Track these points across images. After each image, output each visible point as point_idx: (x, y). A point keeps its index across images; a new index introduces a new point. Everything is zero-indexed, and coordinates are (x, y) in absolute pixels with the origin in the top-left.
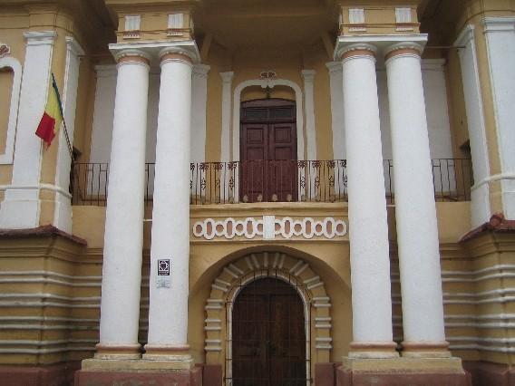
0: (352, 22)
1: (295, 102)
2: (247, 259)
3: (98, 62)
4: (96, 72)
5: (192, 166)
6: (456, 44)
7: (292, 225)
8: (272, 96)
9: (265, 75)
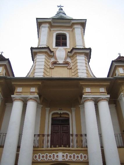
1: (69, 118)
3: (7, 103)
4: (6, 105)
5: (35, 135)
6: (119, 98)
7: (69, 156)
8: (62, 116)
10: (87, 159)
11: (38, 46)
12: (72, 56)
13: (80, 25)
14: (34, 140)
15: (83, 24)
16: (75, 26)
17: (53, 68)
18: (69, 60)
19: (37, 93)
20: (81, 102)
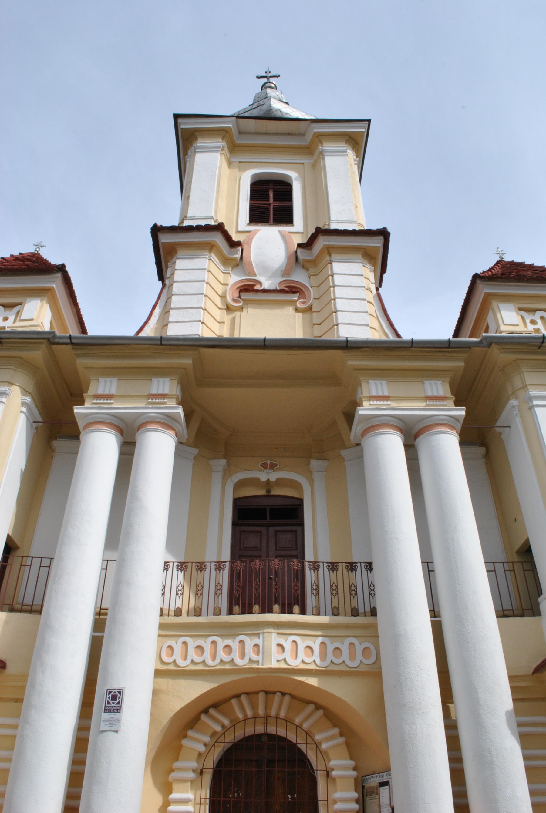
0: (374, 393)
1: (301, 500)
2: (234, 701)
3: (56, 439)
8: (275, 492)
9: (265, 466)
10: (372, 660)
11: (180, 224)
12: (314, 262)
13: (343, 144)
14: (164, 586)
15: (355, 137)
16: (327, 146)
17: (241, 309)
18: (300, 277)
19: (177, 399)
20: (349, 435)
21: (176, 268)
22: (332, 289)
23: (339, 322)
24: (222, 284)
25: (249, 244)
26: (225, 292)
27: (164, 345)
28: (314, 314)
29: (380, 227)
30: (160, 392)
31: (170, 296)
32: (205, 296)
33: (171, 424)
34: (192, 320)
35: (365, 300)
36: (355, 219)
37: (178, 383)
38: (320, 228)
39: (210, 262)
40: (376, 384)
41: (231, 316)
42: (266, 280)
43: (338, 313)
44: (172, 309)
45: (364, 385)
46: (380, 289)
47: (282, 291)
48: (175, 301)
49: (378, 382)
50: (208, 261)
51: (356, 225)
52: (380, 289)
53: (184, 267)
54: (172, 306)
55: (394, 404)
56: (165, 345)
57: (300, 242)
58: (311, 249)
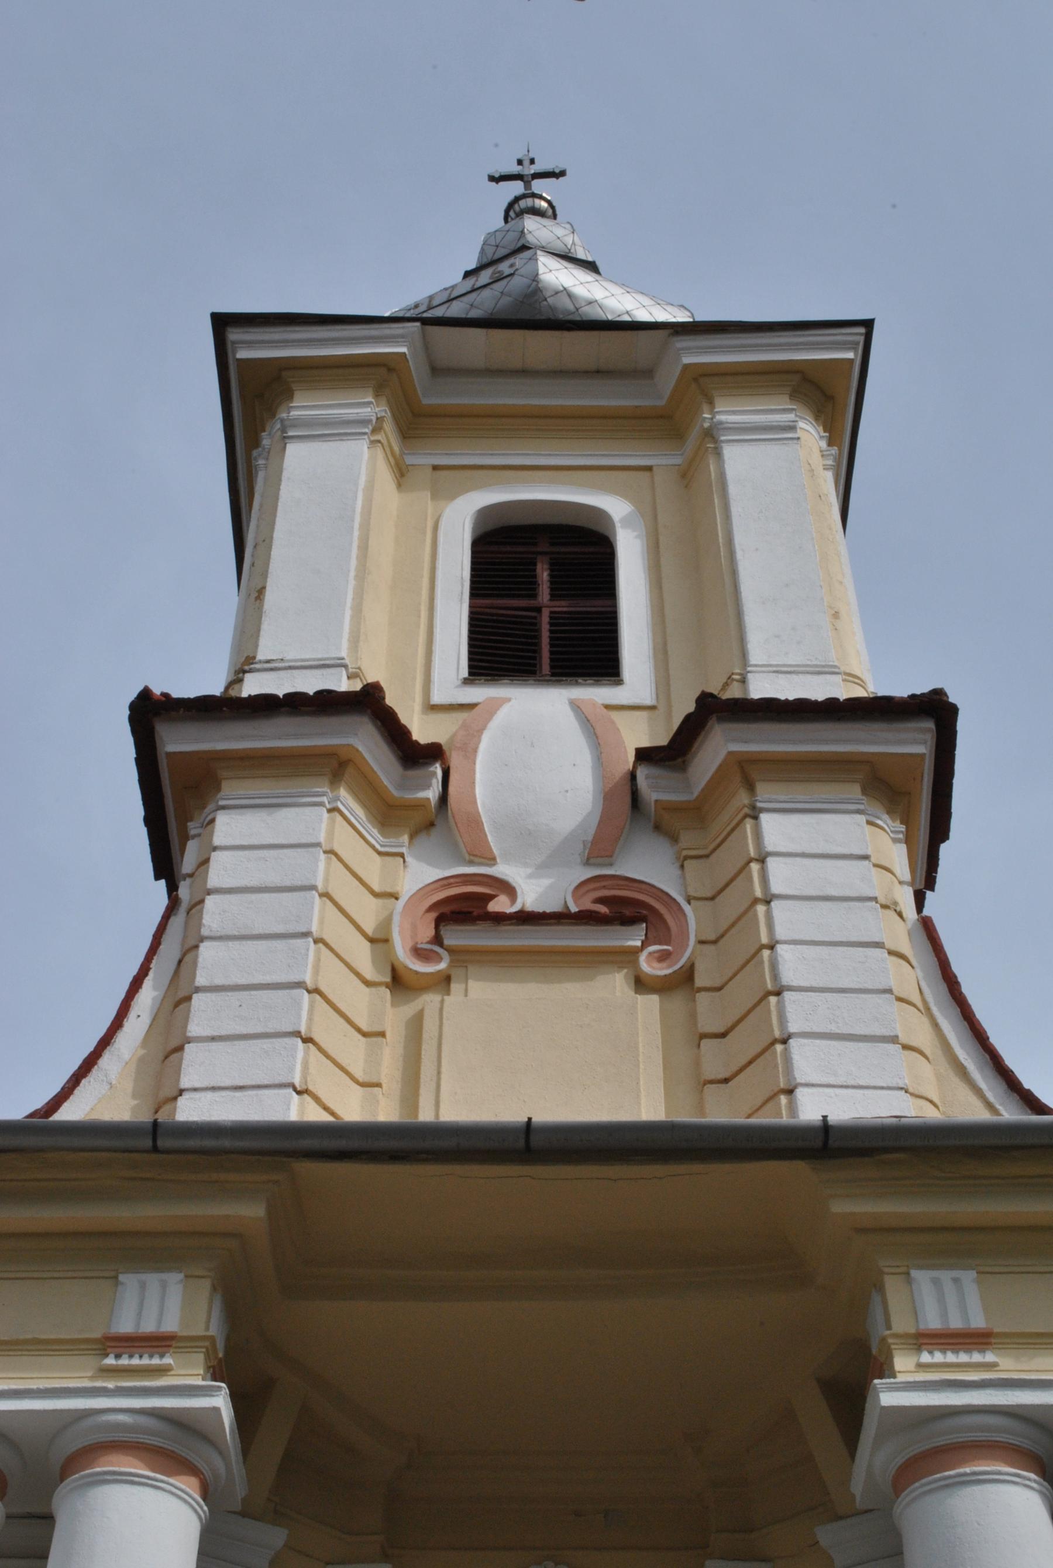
0: (932, 1322)
11: (227, 688)
12: (698, 811)
15: (823, 378)
16: (730, 412)
17: (444, 981)
21: (217, 841)
22: (761, 909)
23: (793, 1028)
24: (376, 895)
25: (470, 752)
26: (386, 923)
27: (162, 1150)
28: (702, 998)
29: (922, 688)
30: (149, 1327)
31: (191, 942)
32: (316, 941)
33: (184, 1453)
34: (270, 1029)
35: (878, 945)
36: (833, 658)
37: (214, 1288)
38: (711, 695)
39: (332, 821)
40: (936, 1282)
41: (409, 1010)
42: (530, 876)
43: (787, 995)
44: (198, 990)
45: (892, 1285)
46: (929, 894)
47: (585, 918)
48: (212, 962)
49: (946, 1276)
50: (326, 815)
51: (838, 679)
52: (929, 894)
53: (245, 838)
54: (201, 980)
55: (1007, 1364)
56: (168, 1152)
57: (645, 743)
58: (683, 768)
